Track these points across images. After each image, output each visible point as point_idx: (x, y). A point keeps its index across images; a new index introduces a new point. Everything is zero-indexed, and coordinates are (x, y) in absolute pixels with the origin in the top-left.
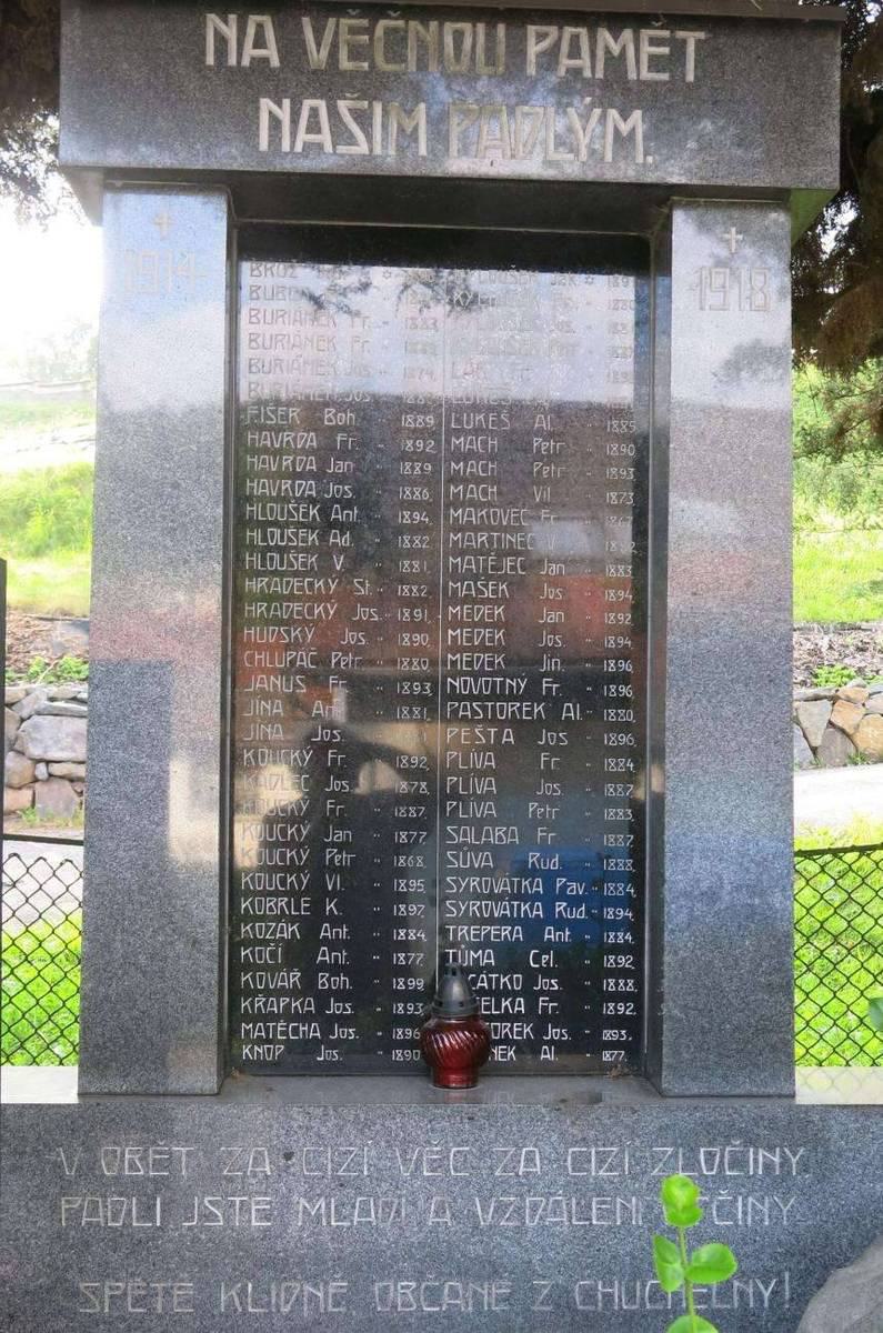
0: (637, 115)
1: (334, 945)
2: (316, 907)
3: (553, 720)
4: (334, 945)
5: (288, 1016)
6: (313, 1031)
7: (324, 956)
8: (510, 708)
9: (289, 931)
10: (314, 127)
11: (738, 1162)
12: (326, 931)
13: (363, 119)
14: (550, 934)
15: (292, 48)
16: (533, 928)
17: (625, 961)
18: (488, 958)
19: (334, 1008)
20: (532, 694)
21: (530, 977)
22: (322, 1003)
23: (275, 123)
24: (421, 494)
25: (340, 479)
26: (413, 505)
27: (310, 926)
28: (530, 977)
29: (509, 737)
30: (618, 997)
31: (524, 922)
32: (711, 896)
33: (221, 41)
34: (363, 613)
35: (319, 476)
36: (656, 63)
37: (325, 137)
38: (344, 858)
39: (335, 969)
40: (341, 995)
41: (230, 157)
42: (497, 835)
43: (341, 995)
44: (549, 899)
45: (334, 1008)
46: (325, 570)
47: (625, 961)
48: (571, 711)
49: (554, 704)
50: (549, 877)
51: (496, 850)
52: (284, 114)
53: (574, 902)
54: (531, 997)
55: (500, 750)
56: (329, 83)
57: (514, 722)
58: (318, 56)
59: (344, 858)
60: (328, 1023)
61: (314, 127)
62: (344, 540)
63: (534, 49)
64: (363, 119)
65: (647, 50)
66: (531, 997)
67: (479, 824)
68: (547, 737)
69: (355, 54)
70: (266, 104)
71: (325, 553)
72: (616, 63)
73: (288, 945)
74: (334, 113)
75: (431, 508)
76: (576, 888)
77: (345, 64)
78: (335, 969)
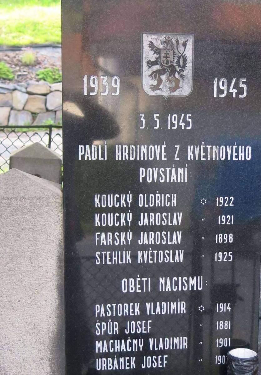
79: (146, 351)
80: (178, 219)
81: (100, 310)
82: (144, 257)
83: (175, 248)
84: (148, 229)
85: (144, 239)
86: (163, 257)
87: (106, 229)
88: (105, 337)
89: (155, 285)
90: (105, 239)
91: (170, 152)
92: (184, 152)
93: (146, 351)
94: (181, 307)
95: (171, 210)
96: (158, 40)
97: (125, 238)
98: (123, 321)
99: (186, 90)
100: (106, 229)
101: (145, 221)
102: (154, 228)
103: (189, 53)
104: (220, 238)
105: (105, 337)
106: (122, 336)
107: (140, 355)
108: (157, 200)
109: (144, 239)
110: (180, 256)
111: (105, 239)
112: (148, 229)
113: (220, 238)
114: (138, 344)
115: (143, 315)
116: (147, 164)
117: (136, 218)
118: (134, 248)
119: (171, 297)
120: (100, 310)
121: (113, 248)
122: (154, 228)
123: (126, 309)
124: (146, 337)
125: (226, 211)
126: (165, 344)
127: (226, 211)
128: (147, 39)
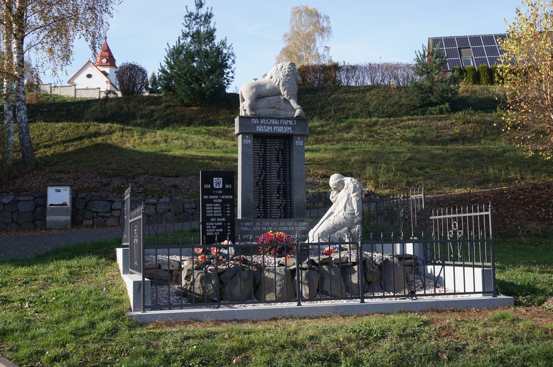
1: (262, 206)
2: (260, 202)
3: (282, 184)
4: (262, 206)
5: (257, 213)
6: (259, 215)
7: (261, 207)
9: (257, 205)
11: (302, 224)
12: (261, 205)
13: (266, 128)
14: (282, 205)
15: (260, 122)
16: (280, 204)
17: (290, 208)
18: (276, 207)
19: (262, 212)
20: (280, 181)
21: (280, 209)
22: (261, 212)
24: (269, 162)
27: (259, 204)
28: (280, 209)
29: (278, 186)
30: (289, 211)
31: (280, 204)
32: (299, 200)
34: (263, 173)
35: (259, 160)
36: (292, 123)
37: (263, 130)
38: (262, 198)
39: (262, 209)
40: (262, 211)
41: (254, 132)
42: (277, 195)
43: (262, 211)
44: (282, 202)
45: (262, 212)
46: (260, 169)
47: (290, 208)
48: (284, 183)
49: (282, 182)
50: (282, 199)
54: (281, 211)
55: (277, 187)
56: (263, 125)
58: (262, 123)
59: (262, 198)
60: (261, 214)
63: (281, 121)
64: (266, 128)
66: (281, 211)
68: (281, 186)
69: (265, 122)
70: (257, 127)
71: (260, 167)
72: (288, 123)
73: (257, 206)
75: (270, 163)
76: (285, 200)
78: (262, 209)
79: (215, 231)
80: (220, 208)
81: (207, 224)
82: (215, 215)
83: (220, 213)
84: (215, 210)
85: (215, 212)
86: (218, 215)
87: (208, 210)
88: (208, 229)
89: (217, 220)
90: (208, 212)
91: (219, 197)
92: (221, 197)
93: (215, 231)
94: (221, 224)
95: (219, 207)
96: (216, 179)
97: (211, 211)
98: (211, 226)
99: (221, 187)
100: (208, 210)
101: (215, 208)
102: (216, 210)
103: (221, 181)
104: (228, 212)
105: (208, 229)
106: (211, 229)
107: (214, 232)
108: (217, 205)
109: (215, 212)
110: (221, 215)
111: (208, 212)
112: (215, 210)
113: (228, 212)
114: (214, 230)
115: (215, 225)
116: (215, 199)
117: (213, 208)
118: (213, 213)
119: (219, 222)
120: (207, 224)
121: (209, 213)
122: (216, 210)
123: (212, 224)
124: (215, 229)
125: (228, 207)
126: (219, 230)
127: (228, 207)
128: (214, 179)
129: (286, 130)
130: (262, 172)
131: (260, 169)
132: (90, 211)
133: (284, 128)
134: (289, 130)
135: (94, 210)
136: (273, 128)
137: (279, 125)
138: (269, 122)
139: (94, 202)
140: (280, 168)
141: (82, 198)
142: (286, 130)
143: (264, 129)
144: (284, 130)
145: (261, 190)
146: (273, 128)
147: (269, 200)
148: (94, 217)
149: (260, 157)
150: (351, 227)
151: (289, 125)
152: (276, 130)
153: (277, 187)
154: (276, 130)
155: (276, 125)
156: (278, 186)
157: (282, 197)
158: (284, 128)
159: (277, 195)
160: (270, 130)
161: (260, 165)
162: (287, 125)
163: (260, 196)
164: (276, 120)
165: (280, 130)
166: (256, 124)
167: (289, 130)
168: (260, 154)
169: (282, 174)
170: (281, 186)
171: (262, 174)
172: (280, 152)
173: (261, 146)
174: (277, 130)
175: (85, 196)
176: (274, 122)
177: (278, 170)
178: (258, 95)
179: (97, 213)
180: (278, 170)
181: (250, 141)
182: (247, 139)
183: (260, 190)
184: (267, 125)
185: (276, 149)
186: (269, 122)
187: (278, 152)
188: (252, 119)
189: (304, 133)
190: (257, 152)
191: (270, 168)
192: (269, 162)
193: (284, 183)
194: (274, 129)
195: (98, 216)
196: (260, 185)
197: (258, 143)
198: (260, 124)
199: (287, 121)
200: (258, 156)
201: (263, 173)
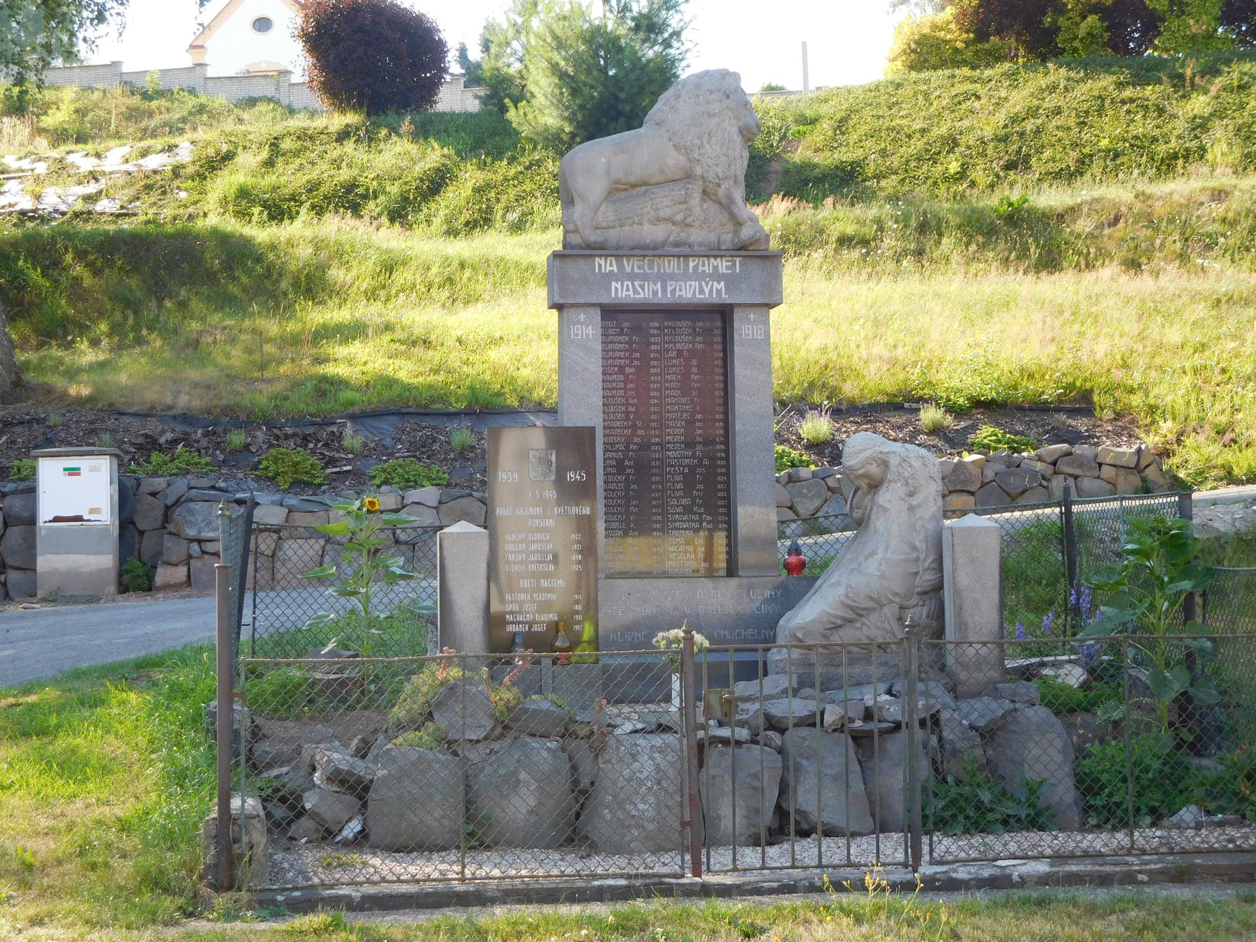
0: (722, 284)
8: (687, 461)
10: (628, 290)
13: (642, 287)
15: (620, 267)
20: (693, 456)
23: (616, 289)
24: (657, 394)
25: (631, 390)
26: (654, 398)
29: (686, 470)
33: (600, 266)
35: (625, 389)
36: (727, 267)
37: (631, 293)
41: (604, 299)
42: (684, 501)
46: (627, 419)
51: (684, 507)
52: (619, 286)
53: (709, 522)
55: (683, 473)
56: (632, 277)
57: (688, 466)
58: (628, 269)
61: (628, 290)
62: (633, 409)
63: (691, 265)
64: (642, 287)
65: (725, 264)
67: (678, 498)
68: (699, 470)
69: (639, 268)
70: (614, 284)
72: (716, 268)
74: (633, 285)
76: (709, 518)
77: (636, 270)
129: (707, 291)
130: (634, 427)
131: (627, 419)
132: (176, 535)
133: (700, 285)
134: (719, 292)
135: (191, 533)
136: (664, 289)
137: (686, 277)
138: (651, 268)
139: (192, 505)
140: (693, 415)
141: (154, 494)
142: (707, 291)
143: (636, 292)
144: (702, 291)
145: (632, 487)
146: (664, 289)
147: (659, 518)
148: (190, 557)
149: (626, 382)
150: (905, 603)
151: (716, 276)
152: (674, 290)
153: (683, 473)
154: (674, 290)
155: (673, 277)
156: (686, 470)
157: (700, 507)
158: (700, 285)
159: (684, 501)
160: (655, 293)
161: (627, 404)
162: (710, 276)
163: (627, 505)
164: (674, 262)
165: (690, 292)
166: (610, 277)
167: (719, 292)
168: (628, 370)
169: (699, 432)
170: (699, 470)
171: (634, 434)
172: (694, 362)
173: (630, 343)
174: (678, 293)
175: (164, 486)
176: (671, 266)
177: (687, 422)
178: (617, 182)
179: (200, 541)
180: (687, 422)
181: (590, 331)
182: (582, 324)
183: (627, 489)
184: (644, 277)
185: (680, 353)
186: (651, 268)
187: (688, 360)
188: (597, 259)
189: (766, 301)
190: (617, 362)
191: (660, 413)
192: (657, 394)
193: (706, 462)
194: (669, 289)
195: (204, 552)
196: (628, 471)
197: (621, 333)
198: (622, 276)
199: (712, 260)
200: (621, 377)
201: (639, 432)
